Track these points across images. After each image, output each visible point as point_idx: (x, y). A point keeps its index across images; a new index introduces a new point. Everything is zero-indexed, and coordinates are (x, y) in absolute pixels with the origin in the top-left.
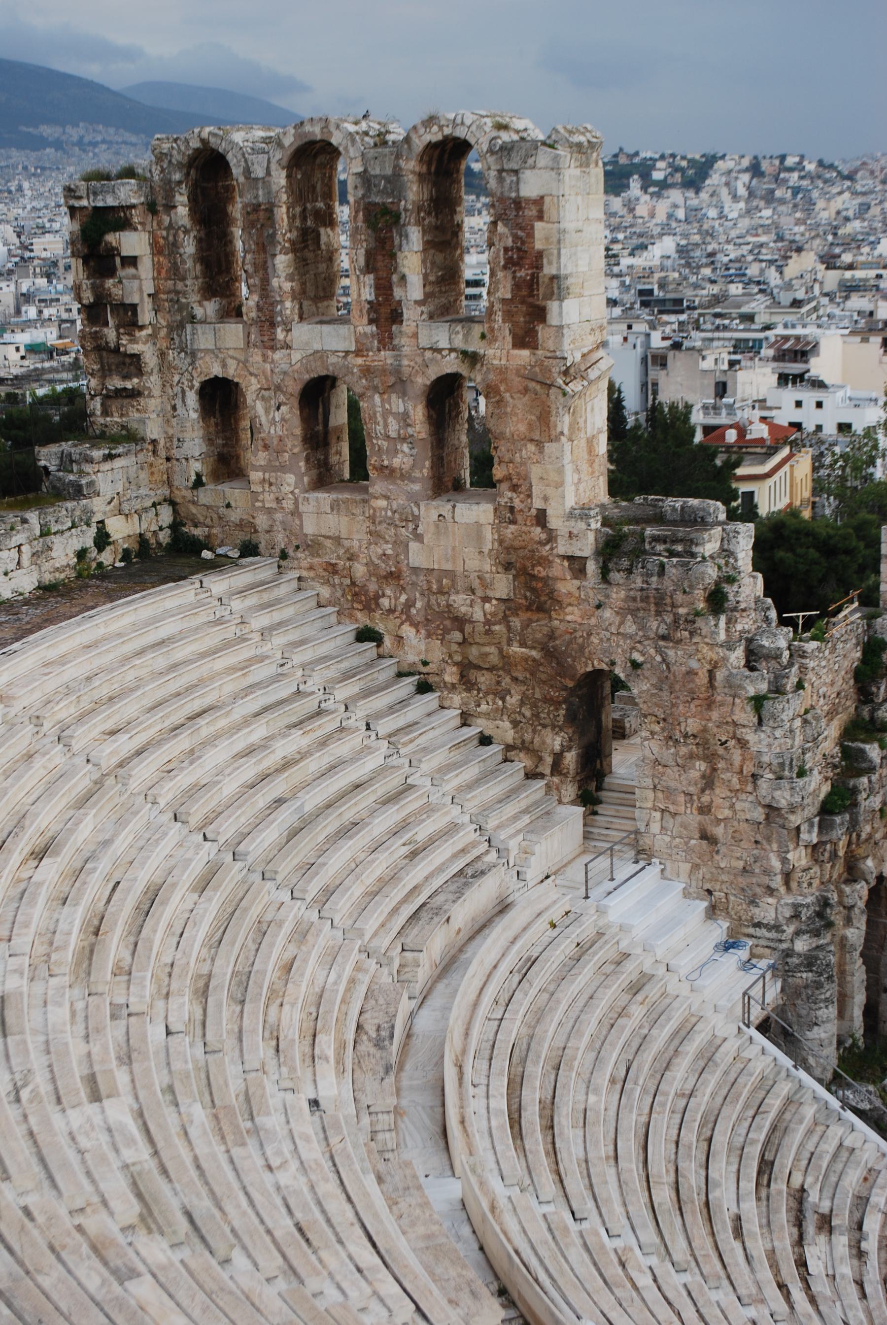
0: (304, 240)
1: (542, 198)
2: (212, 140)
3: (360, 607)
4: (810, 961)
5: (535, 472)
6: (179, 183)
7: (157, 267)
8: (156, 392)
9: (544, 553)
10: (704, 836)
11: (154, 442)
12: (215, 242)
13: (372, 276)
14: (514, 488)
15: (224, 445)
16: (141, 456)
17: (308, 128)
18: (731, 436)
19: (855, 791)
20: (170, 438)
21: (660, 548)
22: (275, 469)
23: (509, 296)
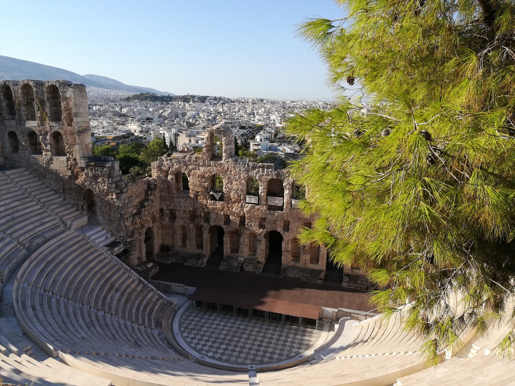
4: (130, 243)
10: (110, 220)
18: (186, 150)
19: (141, 211)
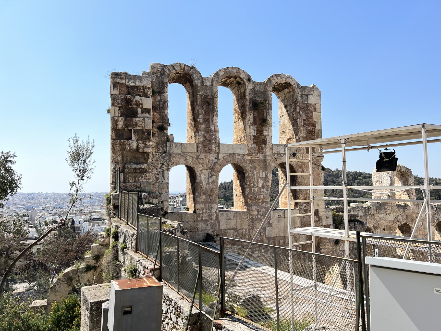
1: (316, 104)
13: (255, 127)
17: (230, 70)
22: (209, 203)
23: (305, 136)
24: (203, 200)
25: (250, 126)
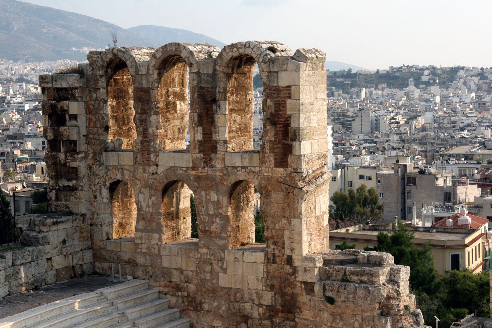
0: (167, 108)
2: (119, 54)
3: (192, 309)
5: (287, 233)
6: (101, 76)
7: (89, 120)
8: (86, 188)
9: (292, 281)
11: (83, 215)
12: (121, 108)
14: (275, 243)
15: (123, 218)
16: (75, 224)
17: (169, 49)
20: (93, 214)
21: (355, 278)
22: (148, 231)
23: (273, 139)
24: (141, 227)
25: (194, 127)
